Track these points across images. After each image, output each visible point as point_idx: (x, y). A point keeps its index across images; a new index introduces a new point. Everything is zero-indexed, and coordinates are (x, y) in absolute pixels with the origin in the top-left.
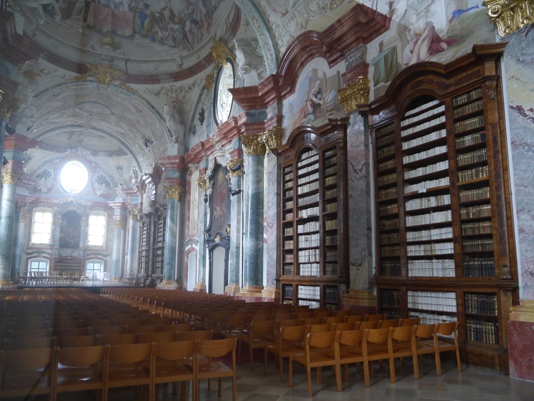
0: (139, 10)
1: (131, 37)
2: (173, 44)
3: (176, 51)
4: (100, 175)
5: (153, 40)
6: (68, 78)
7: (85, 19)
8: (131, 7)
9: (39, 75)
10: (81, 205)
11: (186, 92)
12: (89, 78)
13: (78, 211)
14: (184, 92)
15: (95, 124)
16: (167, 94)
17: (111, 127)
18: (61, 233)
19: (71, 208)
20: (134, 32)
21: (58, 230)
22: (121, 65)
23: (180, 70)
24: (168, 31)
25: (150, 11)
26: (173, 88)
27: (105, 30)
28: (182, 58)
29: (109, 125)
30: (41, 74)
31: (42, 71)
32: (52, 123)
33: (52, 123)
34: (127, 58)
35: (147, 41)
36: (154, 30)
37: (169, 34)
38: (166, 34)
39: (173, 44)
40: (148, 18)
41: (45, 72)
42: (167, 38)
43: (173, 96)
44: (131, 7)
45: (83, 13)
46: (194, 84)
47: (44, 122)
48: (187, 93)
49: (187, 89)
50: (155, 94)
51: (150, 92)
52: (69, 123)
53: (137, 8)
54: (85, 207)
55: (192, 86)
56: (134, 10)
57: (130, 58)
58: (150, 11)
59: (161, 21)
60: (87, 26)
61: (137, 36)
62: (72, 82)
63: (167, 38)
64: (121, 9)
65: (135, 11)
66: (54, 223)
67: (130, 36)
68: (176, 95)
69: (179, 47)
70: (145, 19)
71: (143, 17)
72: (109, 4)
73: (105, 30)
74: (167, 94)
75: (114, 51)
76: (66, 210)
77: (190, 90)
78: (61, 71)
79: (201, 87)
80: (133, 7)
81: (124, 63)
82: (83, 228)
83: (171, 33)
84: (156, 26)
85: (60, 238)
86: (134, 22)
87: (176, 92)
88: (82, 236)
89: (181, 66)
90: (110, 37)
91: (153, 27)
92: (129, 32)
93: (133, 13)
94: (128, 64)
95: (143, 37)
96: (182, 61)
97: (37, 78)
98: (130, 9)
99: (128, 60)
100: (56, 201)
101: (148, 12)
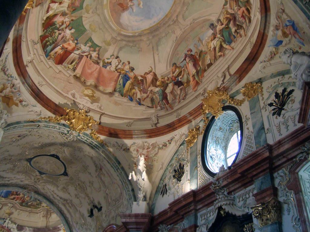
0: (124, 72)
1: (111, 94)
2: (150, 105)
3: (152, 111)
5: (131, 100)
6: (43, 117)
7: (74, 70)
8: (117, 68)
9: (17, 105)
11: (159, 148)
12: (63, 122)
14: (156, 149)
16: (137, 151)
23: (154, 127)
24: (147, 93)
26: (146, 144)
27: (88, 83)
28: (158, 118)
30: (19, 104)
31: (21, 101)
35: (125, 100)
36: (133, 91)
37: (148, 96)
38: (145, 95)
39: (150, 105)
40: (131, 80)
41: (24, 103)
42: (145, 99)
43: (144, 153)
44: (117, 68)
45: (74, 64)
46: (170, 142)
48: (160, 151)
49: (161, 146)
50: (124, 150)
51: (119, 146)
53: (123, 70)
55: (167, 143)
56: (119, 71)
57: (105, 113)
58: (134, 74)
59: (143, 83)
60: (74, 75)
61: (117, 94)
62: (46, 122)
63: (145, 99)
64: (108, 68)
65: (120, 73)
67: (110, 93)
68: (148, 152)
69: (156, 107)
70: (127, 80)
71: (126, 78)
72: (99, 61)
73: (88, 83)
74: (137, 151)
75: (92, 103)
77: (164, 147)
78: (39, 108)
79: (179, 143)
80: (119, 69)
83: (150, 95)
86: (116, 81)
87: (148, 149)
89: (156, 124)
90: (92, 90)
92: (110, 89)
93: (118, 74)
94: (102, 117)
95: (122, 96)
96: (158, 120)
97: (14, 107)
98: (116, 70)
101: (131, 75)
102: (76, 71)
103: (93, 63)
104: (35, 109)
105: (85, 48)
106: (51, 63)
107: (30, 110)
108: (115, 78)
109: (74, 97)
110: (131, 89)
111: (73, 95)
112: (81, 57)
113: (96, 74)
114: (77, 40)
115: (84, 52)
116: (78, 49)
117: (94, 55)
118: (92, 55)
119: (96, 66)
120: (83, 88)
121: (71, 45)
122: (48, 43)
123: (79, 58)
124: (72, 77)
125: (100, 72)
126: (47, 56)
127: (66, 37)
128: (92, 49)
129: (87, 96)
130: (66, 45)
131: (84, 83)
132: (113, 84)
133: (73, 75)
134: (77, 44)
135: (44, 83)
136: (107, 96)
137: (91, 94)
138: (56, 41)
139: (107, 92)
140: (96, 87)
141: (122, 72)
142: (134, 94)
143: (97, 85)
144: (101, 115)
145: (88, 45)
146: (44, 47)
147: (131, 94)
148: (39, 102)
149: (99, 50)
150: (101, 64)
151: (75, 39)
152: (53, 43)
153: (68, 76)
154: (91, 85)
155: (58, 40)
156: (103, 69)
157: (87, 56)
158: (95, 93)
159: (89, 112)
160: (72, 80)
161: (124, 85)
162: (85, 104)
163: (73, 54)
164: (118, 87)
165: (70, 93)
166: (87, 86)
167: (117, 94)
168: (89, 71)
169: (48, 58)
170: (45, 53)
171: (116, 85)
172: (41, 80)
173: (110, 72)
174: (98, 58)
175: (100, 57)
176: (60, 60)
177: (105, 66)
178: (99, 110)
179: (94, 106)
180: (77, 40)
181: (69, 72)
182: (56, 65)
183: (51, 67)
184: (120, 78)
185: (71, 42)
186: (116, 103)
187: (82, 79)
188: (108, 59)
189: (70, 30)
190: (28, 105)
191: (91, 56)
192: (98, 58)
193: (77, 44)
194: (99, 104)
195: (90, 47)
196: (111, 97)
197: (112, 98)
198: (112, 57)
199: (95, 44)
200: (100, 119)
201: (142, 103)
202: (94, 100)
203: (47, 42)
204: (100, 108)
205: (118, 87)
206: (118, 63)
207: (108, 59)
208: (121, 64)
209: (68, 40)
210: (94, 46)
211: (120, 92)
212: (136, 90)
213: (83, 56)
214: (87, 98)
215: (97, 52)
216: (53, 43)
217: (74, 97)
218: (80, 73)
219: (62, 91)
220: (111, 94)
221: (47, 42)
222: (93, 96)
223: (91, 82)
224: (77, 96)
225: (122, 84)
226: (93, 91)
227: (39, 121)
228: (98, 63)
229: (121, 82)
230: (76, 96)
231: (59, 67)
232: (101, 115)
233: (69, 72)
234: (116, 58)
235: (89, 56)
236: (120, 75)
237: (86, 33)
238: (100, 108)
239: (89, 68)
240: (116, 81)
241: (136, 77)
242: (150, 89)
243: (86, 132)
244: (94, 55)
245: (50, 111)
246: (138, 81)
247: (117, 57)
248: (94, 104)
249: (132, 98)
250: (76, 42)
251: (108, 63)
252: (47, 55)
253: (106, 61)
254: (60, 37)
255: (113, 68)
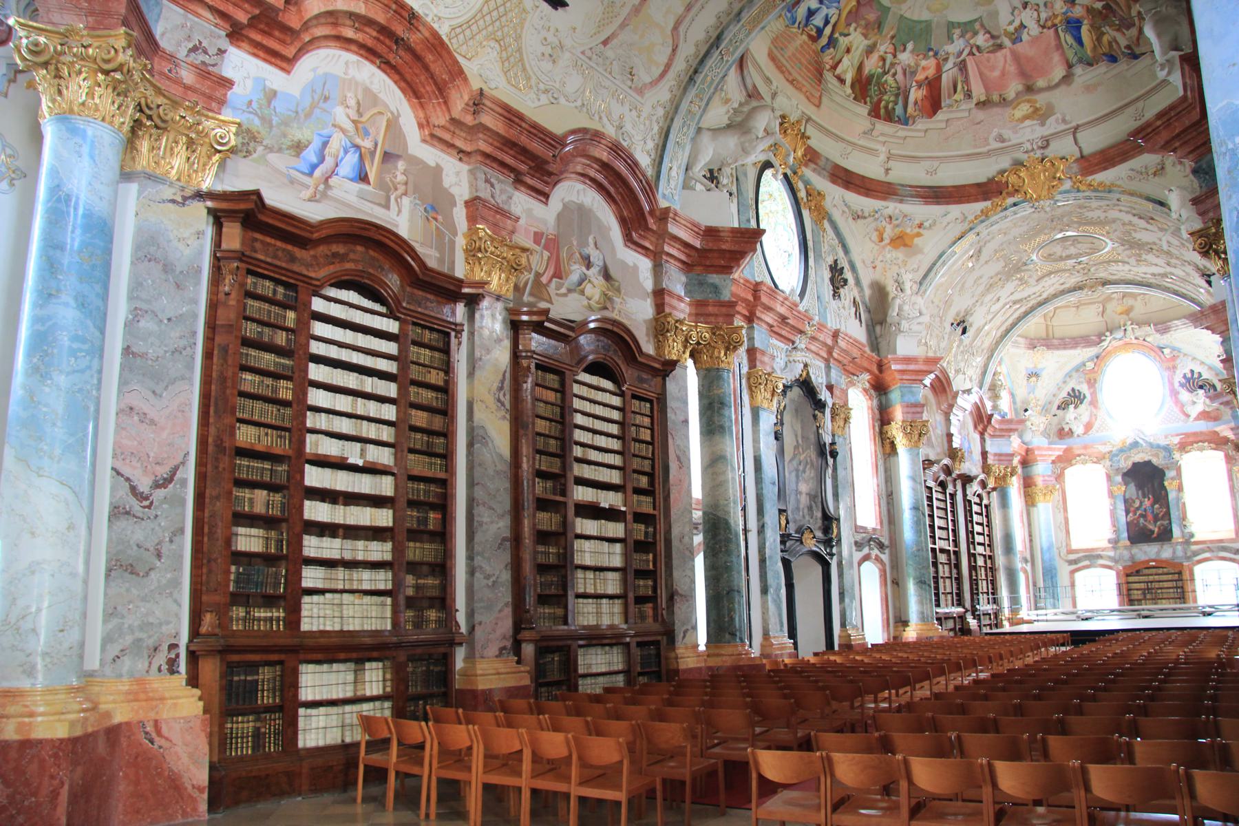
1: (1067, 79)
4: (1187, 371)
5: (1113, 59)
6: (971, 218)
7: (968, 95)
10: (1158, 446)
12: (1010, 201)
13: (1155, 461)
15: (1103, 275)
17: (1135, 269)
18: (1127, 512)
19: (1139, 457)
20: (1070, 66)
21: (1121, 507)
22: (1064, 147)
25: (1082, 6)
29: (1127, 267)
32: (1015, 303)
33: (1015, 303)
34: (1074, 124)
36: (1105, 39)
40: (1085, 22)
42: (1138, 39)
47: (995, 308)
52: (1051, 291)
53: (1055, 16)
54: (1167, 450)
56: (1049, 23)
58: (1082, 6)
61: (1078, 70)
62: (982, 222)
63: (1138, 39)
64: (1025, 37)
65: (1054, 25)
66: (1111, 495)
70: (1079, 28)
71: (1074, 26)
73: (1011, 94)
75: (1043, 124)
76: (1129, 464)
78: (955, 210)
81: (1071, 137)
82: (1172, 496)
84: (1106, 29)
85: (1129, 524)
86: (1059, 46)
88: (1174, 514)
91: (1103, 34)
92: (1059, 72)
94: (1078, 135)
95: (1090, 64)
98: (1043, 27)
99: (1076, 128)
100: (1104, 449)
102: (974, 94)
103: (991, 55)
104: (950, 217)
105: (958, 44)
106: (922, 124)
107: (945, 224)
108: (1053, 43)
109: (1003, 141)
110: (1099, 39)
111: (1001, 139)
112: (962, 67)
113: (1012, 69)
114: (931, 49)
115: (961, 53)
116: (946, 60)
117: (981, 40)
118: (978, 43)
119: (999, 54)
120: (1009, 111)
121: (928, 67)
122: (890, 106)
123: (960, 69)
124: (974, 111)
125: (1016, 57)
126: (907, 124)
127: (909, 66)
128: (968, 36)
129: (1026, 117)
130: (920, 76)
131: (1004, 102)
132: (1056, 57)
133: (973, 105)
134: (936, 54)
135: (936, 164)
136: (1063, 88)
137: (1031, 110)
138: (899, 88)
139: (1057, 80)
140: (1029, 89)
141: (1057, 21)
142: (1110, 43)
143: (1030, 83)
144: (1074, 134)
145: (955, 36)
146: (889, 117)
147: (1105, 49)
148: (948, 203)
149: (982, 26)
150: (1007, 42)
151: (928, 50)
152: (897, 95)
153: (967, 114)
154: (1018, 94)
155: (902, 85)
156: (1019, 47)
157: (971, 54)
158: (1036, 101)
159: (1048, 145)
160: (980, 115)
161: (1079, 41)
162: (1030, 138)
163: (944, 76)
164: (1070, 55)
165: (991, 140)
166: (1012, 101)
167: (1078, 70)
168: (997, 73)
169: (911, 122)
170: (899, 121)
171: (1063, 54)
172: (926, 164)
173: (1035, 40)
174: (993, 37)
175: (995, 33)
176: (933, 104)
177: (1016, 38)
178: (1063, 127)
179: (1052, 126)
180: (931, 49)
181: (963, 107)
182: (934, 119)
183: (926, 131)
184: (1062, 34)
185: (924, 63)
186: (1089, 88)
187: (995, 98)
188: (1011, 23)
189: (904, 50)
190: (935, 222)
191: (978, 48)
192: (993, 37)
193: (936, 54)
194: (1058, 115)
195: (962, 36)
196: (1069, 84)
197: (1074, 85)
198: (1016, 12)
199: (965, 24)
200: (1076, 143)
201: (1137, 51)
202: (1040, 115)
203: (886, 107)
204: (1064, 121)
205: (1070, 55)
206: (1035, 14)
207: (1011, 23)
208: (1042, 8)
209: (917, 65)
210: (968, 28)
211: (1080, 61)
212: (1110, 33)
213: (964, 61)
214: (1028, 122)
215: (982, 32)
216: (897, 95)
217: (1003, 141)
218: (983, 91)
219: (975, 147)
220: (1067, 79)
221: (886, 107)
222: (1036, 110)
223: (1013, 88)
224: (1007, 133)
225: (1075, 44)
226: (1029, 101)
227: (971, 229)
228: (1000, 47)
229: (1070, 40)
230: (1005, 137)
231: (941, 116)
232: (1074, 134)
233: (963, 107)
234: (1025, 8)
235: (974, 50)
236: (1056, 31)
237: (934, 26)
238: (1064, 121)
239: (993, 69)
240: (1059, 46)
241: (1090, 10)
242: (1134, 13)
243: (1063, 188)
244: (981, 40)
245: (976, 200)
246: (1100, 12)
247: (1025, 6)
248: (1048, 122)
249: (1112, 56)
250: (931, 53)
251: (1016, 30)
252: (905, 121)
253: (1011, 29)
254: (900, 77)
255: (1034, 29)
